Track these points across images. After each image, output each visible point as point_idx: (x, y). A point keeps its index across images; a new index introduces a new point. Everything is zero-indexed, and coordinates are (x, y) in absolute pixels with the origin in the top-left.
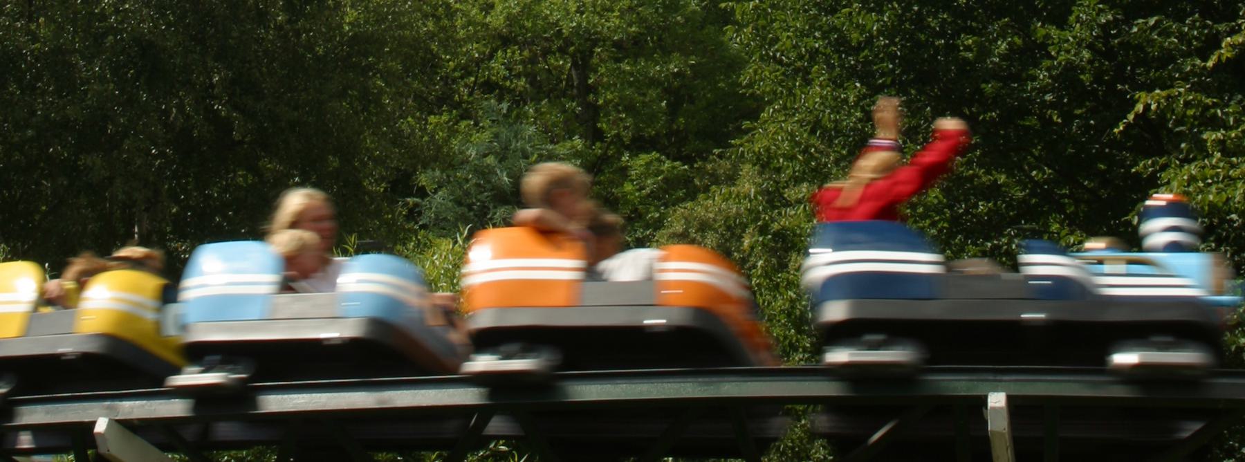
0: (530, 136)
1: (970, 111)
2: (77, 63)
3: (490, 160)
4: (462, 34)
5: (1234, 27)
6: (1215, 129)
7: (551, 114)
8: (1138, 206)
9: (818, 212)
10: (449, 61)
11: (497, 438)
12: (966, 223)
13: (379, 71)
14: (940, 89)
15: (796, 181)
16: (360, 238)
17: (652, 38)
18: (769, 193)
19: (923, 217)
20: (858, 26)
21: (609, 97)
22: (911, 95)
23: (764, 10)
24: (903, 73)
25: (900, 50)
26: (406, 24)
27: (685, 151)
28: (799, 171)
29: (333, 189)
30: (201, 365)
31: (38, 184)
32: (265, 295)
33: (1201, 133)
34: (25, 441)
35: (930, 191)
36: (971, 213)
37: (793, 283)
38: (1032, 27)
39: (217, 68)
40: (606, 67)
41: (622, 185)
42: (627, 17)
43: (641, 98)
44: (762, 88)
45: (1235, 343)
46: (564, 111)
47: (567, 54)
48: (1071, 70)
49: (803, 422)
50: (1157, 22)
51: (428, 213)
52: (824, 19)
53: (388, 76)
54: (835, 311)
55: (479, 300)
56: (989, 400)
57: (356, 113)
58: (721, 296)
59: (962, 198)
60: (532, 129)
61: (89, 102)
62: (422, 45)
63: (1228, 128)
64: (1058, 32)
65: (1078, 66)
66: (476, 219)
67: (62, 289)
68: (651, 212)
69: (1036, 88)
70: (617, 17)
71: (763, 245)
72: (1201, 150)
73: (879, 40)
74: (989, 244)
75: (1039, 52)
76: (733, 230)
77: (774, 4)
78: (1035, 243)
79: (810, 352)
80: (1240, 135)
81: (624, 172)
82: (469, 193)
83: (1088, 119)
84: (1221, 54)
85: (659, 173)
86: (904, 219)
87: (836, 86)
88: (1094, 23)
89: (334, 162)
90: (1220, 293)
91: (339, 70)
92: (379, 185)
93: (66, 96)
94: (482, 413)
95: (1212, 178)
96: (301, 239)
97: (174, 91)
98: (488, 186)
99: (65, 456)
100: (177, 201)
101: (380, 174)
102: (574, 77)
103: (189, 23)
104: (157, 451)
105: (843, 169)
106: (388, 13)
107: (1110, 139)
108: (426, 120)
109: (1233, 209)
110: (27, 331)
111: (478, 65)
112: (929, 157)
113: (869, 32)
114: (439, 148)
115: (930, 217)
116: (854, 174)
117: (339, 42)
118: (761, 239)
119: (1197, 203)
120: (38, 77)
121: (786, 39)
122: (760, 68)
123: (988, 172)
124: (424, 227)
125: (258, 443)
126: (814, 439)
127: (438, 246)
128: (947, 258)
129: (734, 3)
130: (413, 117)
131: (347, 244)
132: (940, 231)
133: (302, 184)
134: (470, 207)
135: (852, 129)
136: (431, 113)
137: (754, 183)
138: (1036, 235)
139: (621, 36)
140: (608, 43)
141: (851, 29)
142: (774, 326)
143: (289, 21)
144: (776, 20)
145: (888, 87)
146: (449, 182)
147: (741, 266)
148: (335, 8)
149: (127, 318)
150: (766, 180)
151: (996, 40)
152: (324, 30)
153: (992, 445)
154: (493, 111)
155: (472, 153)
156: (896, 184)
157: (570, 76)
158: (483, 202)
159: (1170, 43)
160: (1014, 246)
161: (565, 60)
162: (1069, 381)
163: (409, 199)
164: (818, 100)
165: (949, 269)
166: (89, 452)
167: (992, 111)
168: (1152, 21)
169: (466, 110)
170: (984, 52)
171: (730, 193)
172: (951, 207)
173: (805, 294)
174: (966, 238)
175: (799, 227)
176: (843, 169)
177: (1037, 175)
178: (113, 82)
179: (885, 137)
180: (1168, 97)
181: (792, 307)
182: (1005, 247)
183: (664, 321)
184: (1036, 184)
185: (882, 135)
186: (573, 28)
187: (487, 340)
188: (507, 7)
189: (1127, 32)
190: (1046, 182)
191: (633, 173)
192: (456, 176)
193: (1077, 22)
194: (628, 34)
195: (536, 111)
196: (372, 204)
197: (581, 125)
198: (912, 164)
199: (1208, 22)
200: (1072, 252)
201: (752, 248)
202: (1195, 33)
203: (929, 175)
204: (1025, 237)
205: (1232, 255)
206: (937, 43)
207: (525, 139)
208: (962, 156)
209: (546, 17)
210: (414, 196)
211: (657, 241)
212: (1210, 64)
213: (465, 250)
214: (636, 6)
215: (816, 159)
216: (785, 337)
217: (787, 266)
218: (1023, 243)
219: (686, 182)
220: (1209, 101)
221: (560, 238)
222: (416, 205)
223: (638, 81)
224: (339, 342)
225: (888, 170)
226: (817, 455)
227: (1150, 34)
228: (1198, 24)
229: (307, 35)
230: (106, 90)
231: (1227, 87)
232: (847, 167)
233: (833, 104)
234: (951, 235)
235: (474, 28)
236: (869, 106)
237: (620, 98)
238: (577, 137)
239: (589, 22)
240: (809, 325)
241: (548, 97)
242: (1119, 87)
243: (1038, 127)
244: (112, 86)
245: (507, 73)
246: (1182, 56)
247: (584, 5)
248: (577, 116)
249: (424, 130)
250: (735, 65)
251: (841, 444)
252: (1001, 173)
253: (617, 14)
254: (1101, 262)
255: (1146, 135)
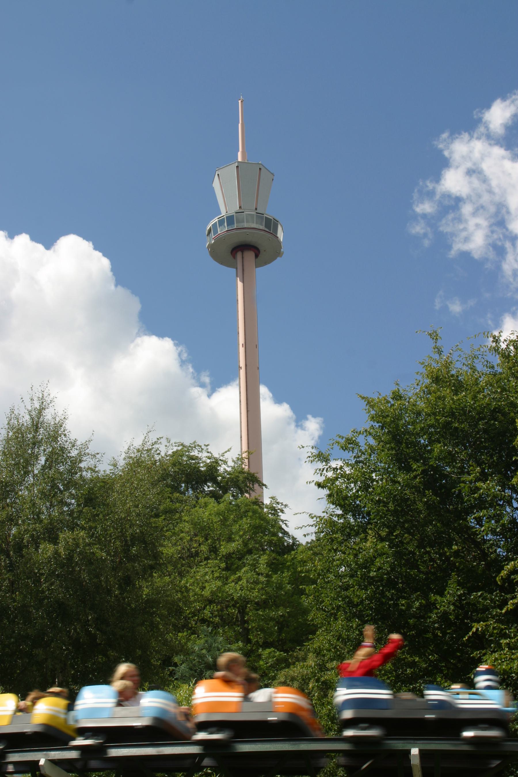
0: (220, 641)
1: (404, 631)
2: (32, 611)
3: (204, 651)
4: (192, 599)
5: (513, 596)
6: (506, 639)
7: (229, 632)
8: (474, 670)
9: (340, 673)
10: (187, 610)
11: (207, 767)
12: (402, 678)
13: (158, 614)
14: (391, 622)
15: (331, 660)
16: (150, 684)
17: (271, 601)
18: (320, 665)
19: (384, 675)
20: (357, 595)
21: (253, 625)
22: (379, 624)
23: (318, 589)
24: (376, 615)
25: (375, 606)
26: (169, 595)
27: (285, 648)
28: (332, 656)
29: (138, 663)
30: (84, 737)
31: (16, 661)
32: (110, 708)
33: (500, 640)
34: (11, 768)
35: (387, 664)
36: (404, 673)
37: (330, 703)
38: (430, 596)
39: (90, 613)
40: (252, 613)
41: (259, 662)
42: (261, 592)
43: (267, 626)
44: (317, 621)
45: (514, 727)
46: (235, 631)
47: (236, 607)
48: (445, 614)
49: (334, 760)
50: (481, 594)
51: (178, 673)
52: (343, 593)
53: (161, 616)
54: (348, 714)
55: (199, 709)
56: (412, 751)
57: (148, 632)
58: (300, 708)
59: (400, 667)
60: (221, 638)
61: (37, 627)
62: (176, 603)
63: (511, 638)
64: (440, 598)
65: (448, 612)
66: (198, 676)
67: (26, 705)
68: (271, 673)
69: (431, 622)
70: (257, 592)
71: (318, 687)
72: (500, 647)
73: (366, 601)
74: (412, 686)
75: (432, 607)
76: (305, 680)
77: (322, 587)
78: (430, 686)
79: (337, 731)
80: (516, 641)
81: (259, 656)
82: (195, 665)
83: (453, 634)
84: (508, 607)
85: (274, 657)
86: (376, 676)
87: (348, 620)
88: (455, 594)
89: (139, 652)
90: (508, 707)
91: (141, 614)
92: (158, 662)
93: (27, 625)
94: (200, 757)
95: (504, 659)
96: (125, 684)
97: (72, 623)
98: (203, 662)
99: (27, 775)
100: (74, 669)
101: (158, 657)
102: (239, 617)
103: (79, 595)
104: (65, 773)
105: (351, 655)
106: (161, 590)
107: (462, 643)
108: (177, 635)
109: (513, 672)
110: (11, 722)
111: (199, 612)
112: (386, 650)
113: (362, 598)
114: (183, 646)
115: (387, 675)
116: (355, 657)
117: (141, 602)
118: (317, 684)
119: (498, 669)
120: (16, 617)
121: (327, 601)
122: (316, 613)
123: (411, 657)
124: (176, 679)
125: (107, 769)
126: (339, 768)
127: (182, 687)
128: (394, 692)
129: (305, 586)
130: (172, 634)
131: (144, 686)
132: (391, 681)
133: (126, 661)
134: (195, 671)
135: (355, 639)
136: (179, 632)
137: (314, 661)
138: (431, 682)
139: (258, 600)
140: (253, 603)
141: (354, 597)
142: (322, 720)
143: (120, 594)
144: (323, 593)
145: (370, 621)
146: (187, 661)
147: (308, 695)
148: (139, 588)
149: (53, 717)
150: (319, 660)
151: (414, 601)
152: (135, 597)
153: (413, 770)
154: (205, 631)
155: (196, 648)
156: (373, 661)
157: (237, 617)
158: (201, 669)
159: (487, 603)
160: (422, 687)
161: (235, 610)
162: (445, 743)
163: (170, 668)
164: (340, 626)
165: (395, 697)
166: (37, 773)
167: (413, 631)
168: (479, 594)
169: (194, 630)
170: (409, 607)
171: (304, 665)
172: (396, 671)
173: (335, 707)
174: (402, 684)
175: (332, 679)
176: (351, 655)
177: (431, 657)
178: (47, 619)
179: (368, 642)
180: (486, 625)
181: (330, 713)
182: (418, 688)
183: (276, 718)
184: (431, 661)
185: (367, 641)
186: (238, 596)
187: (203, 726)
188: (211, 588)
189: (469, 598)
190: (435, 660)
191: (263, 657)
192: (190, 658)
193: (448, 594)
194: (261, 599)
195: (223, 631)
196: (155, 670)
197: (242, 637)
198: (379, 653)
199: (503, 594)
200: (446, 689)
201: (313, 688)
202: (497, 598)
203: (386, 658)
204: (427, 684)
205: (513, 691)
206: (390, 603)
207: (218, 643)
208: (400, 650)
209: (227, 592)
210: (172, 666)
211: (274, 685)
212: (503, 611)
213: (194, 689)
214: (265, 587)
215: (340, 651)
216: (327, 725)
217: (327, 696)
218: (426, 686)
219: (285, 660)
220: (503, 627)
221: (233, 684)
222: (173, 670)
223: (266, 619)
224: (141, 727)
225: (369, 655)
226: (340, 774)
227: (479, 599)
228: (498, 595)
229: (128, 599)
230: (44, 622)
231: (510, 621)
232: (352, 654)
233: (347, 628)
234: (396, 683)
235: (197, 597)
236: (362, 629)
237: (258, 626)
238: (240, 642)
239: (245, 594)
240: (337, 720)
241: (228, 625)
242: (466, 621)
243: (432, 638)
244: (46, 620)
245: (211, 615)
246: (492, 608)
247: (243, 587)
248: (240, 633)
249: (176, 639)
250: (306, 612)
251: (350, 770)
252: (416, 657)
253: (257, 590)
254: (458, 694)
255: (477, 641)
